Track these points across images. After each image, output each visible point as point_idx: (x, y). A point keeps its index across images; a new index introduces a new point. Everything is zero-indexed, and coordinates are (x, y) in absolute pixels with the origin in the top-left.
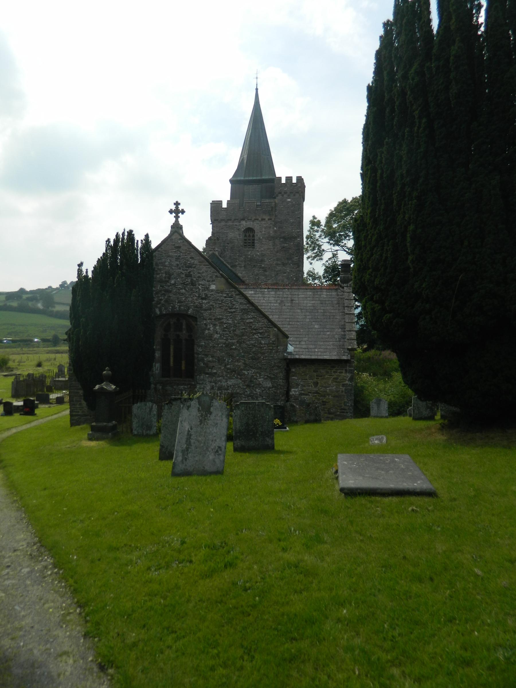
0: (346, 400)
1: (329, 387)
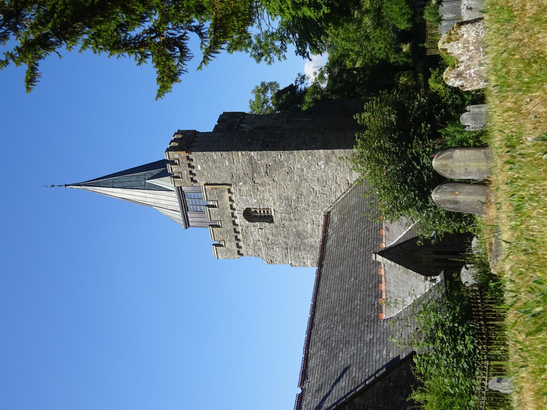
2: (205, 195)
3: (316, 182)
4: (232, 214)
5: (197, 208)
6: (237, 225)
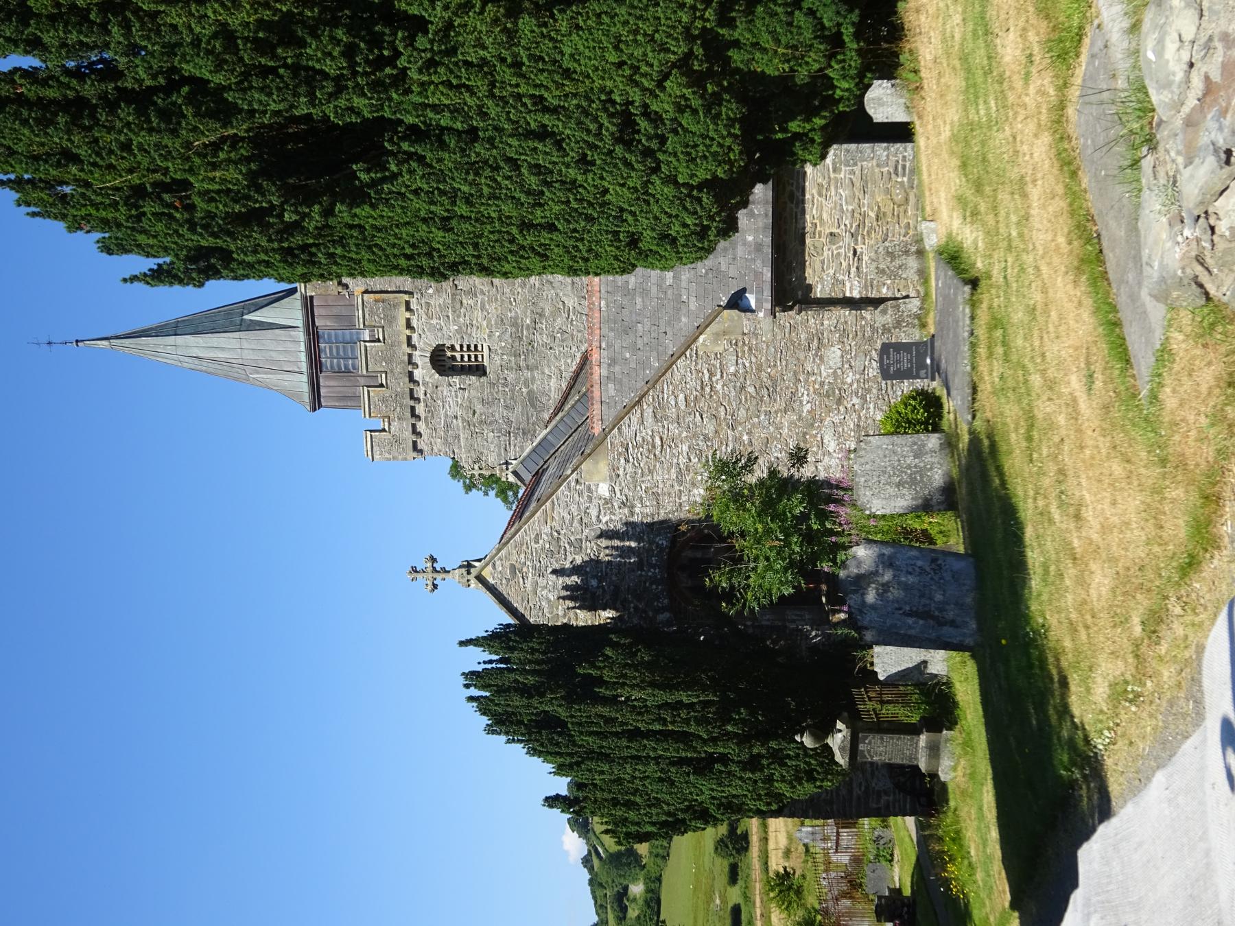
0: (874, 162)
1: (841, 205)
2: (361, 316)
3: (569, 288)
4: (410, 356)
5: (339, 366)
6: (417, 383)
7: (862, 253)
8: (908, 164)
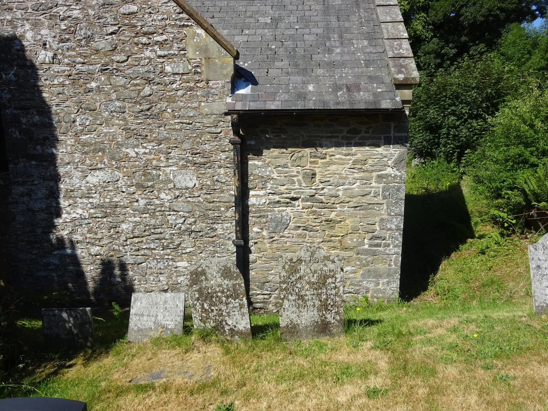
0: (386, 217)
1: (344, 184)
7: (294, 206)
8: (380, 249)
